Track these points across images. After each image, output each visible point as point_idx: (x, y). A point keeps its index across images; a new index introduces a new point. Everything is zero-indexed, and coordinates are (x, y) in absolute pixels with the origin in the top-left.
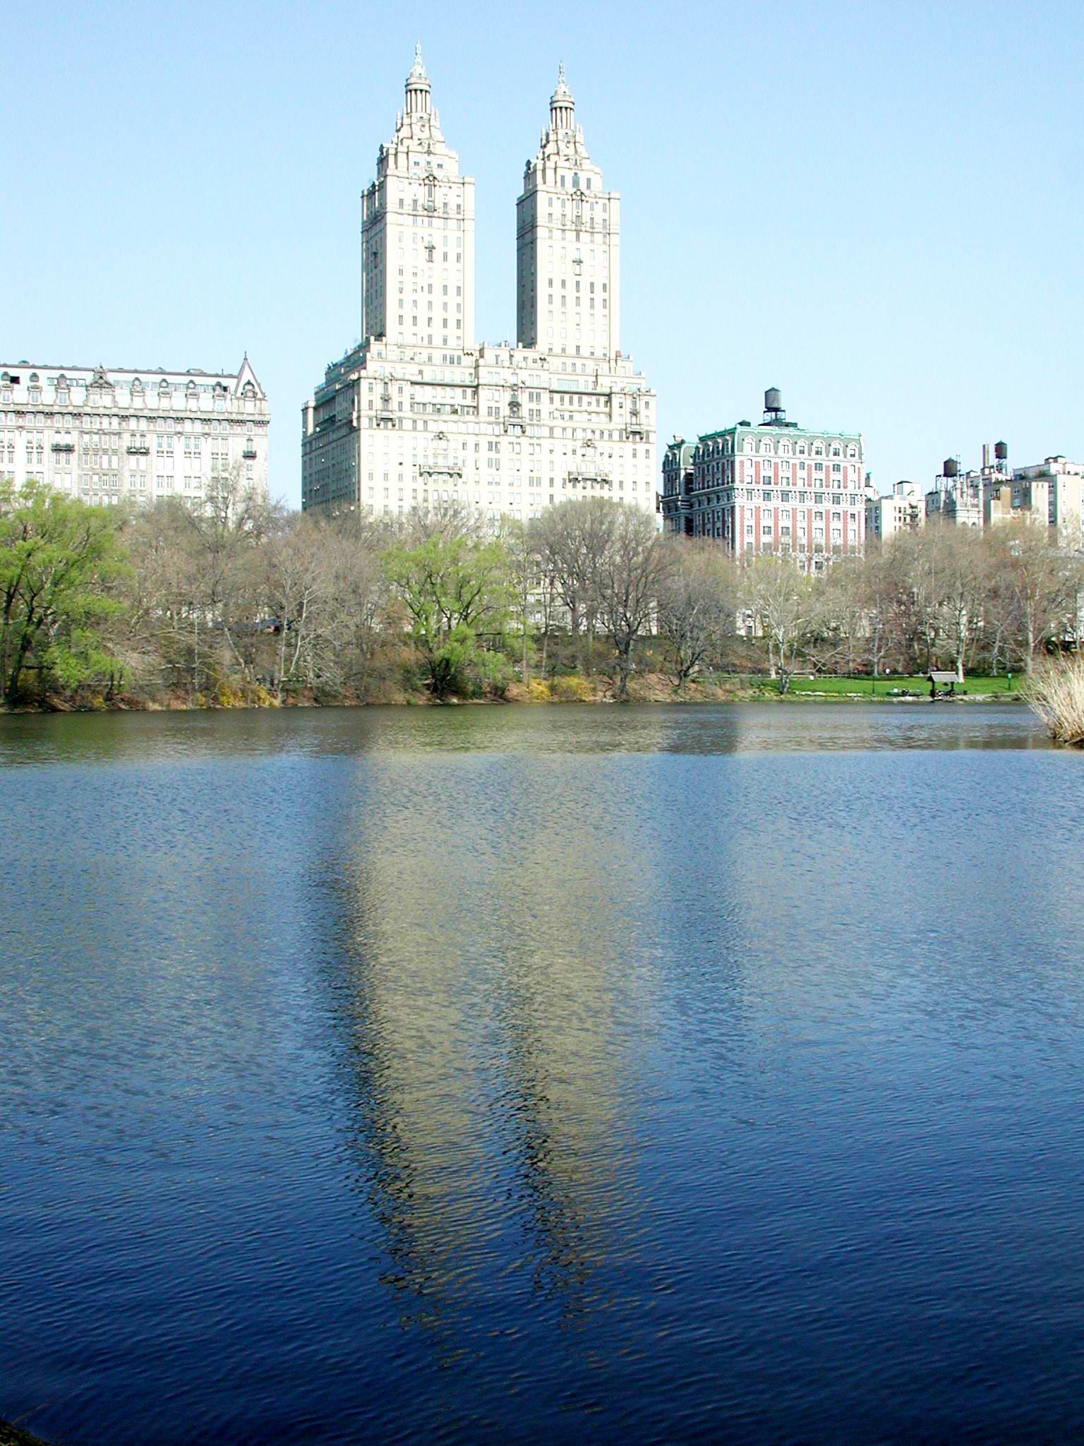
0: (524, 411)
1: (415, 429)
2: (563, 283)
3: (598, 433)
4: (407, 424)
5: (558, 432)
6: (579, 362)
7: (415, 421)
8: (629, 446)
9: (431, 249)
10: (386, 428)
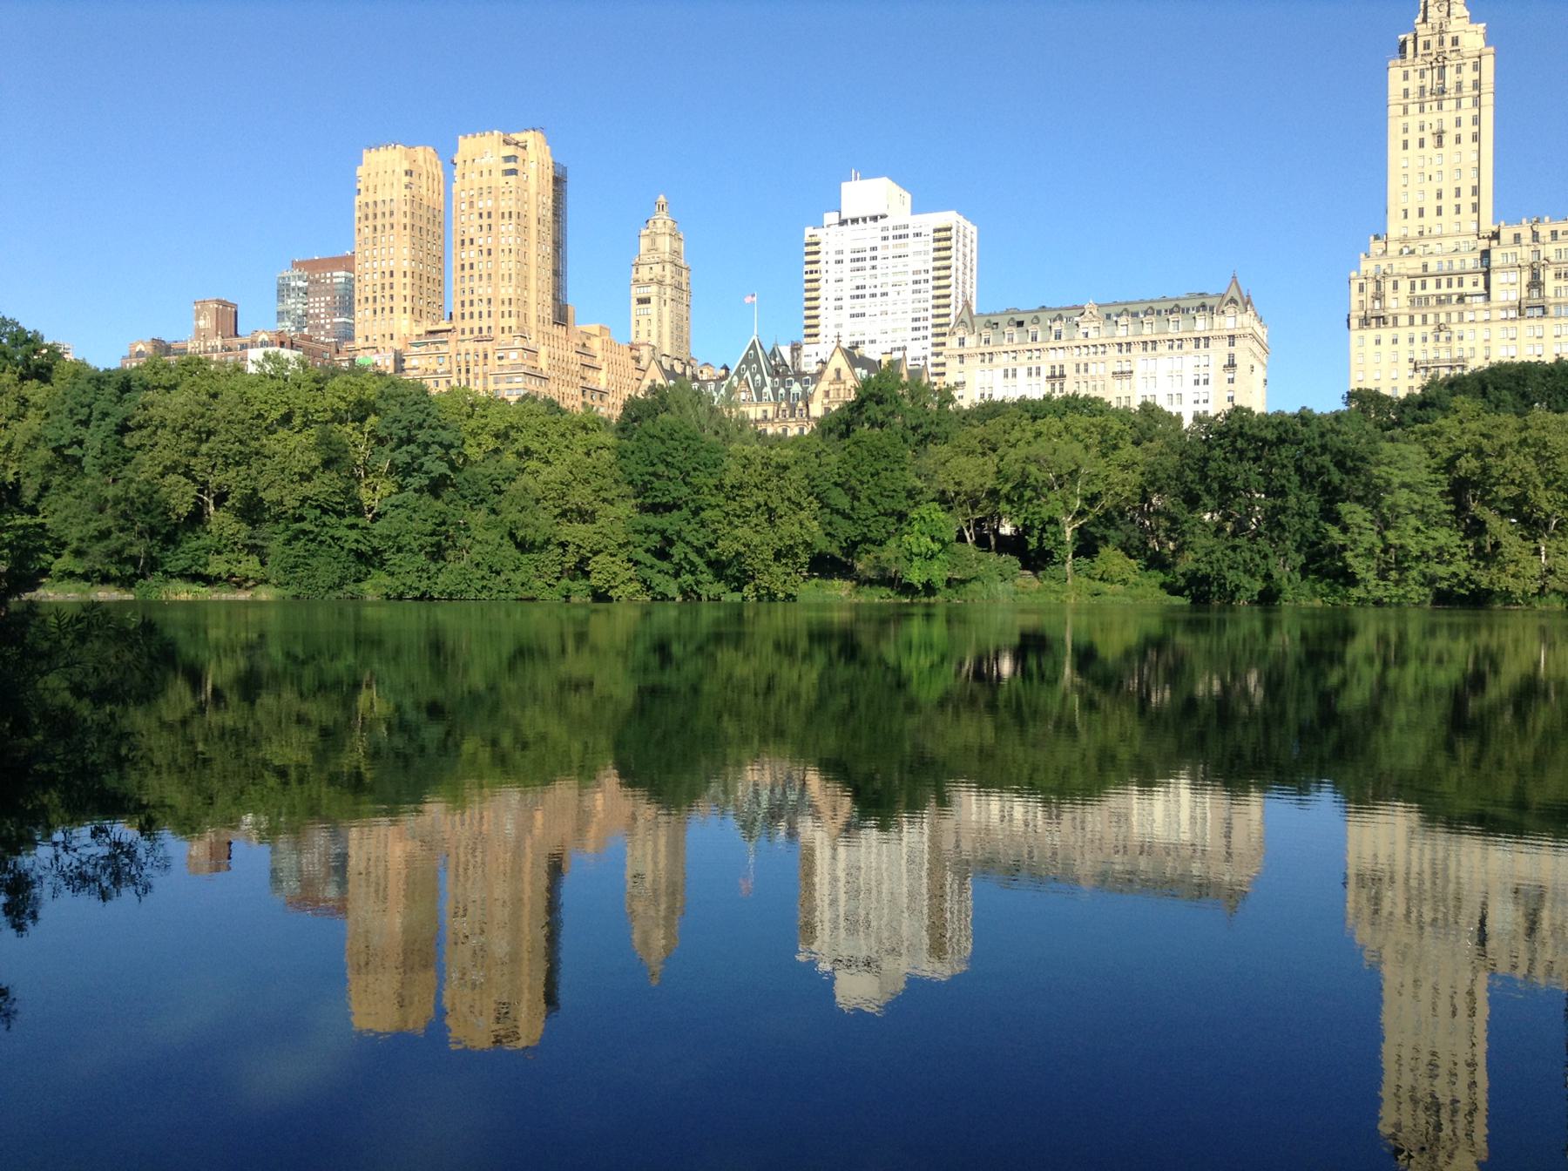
1: (1412, 323)
4: (1403, 320)
7: (1412, 318)
9: (1439, 136)
10: (1378, 326)
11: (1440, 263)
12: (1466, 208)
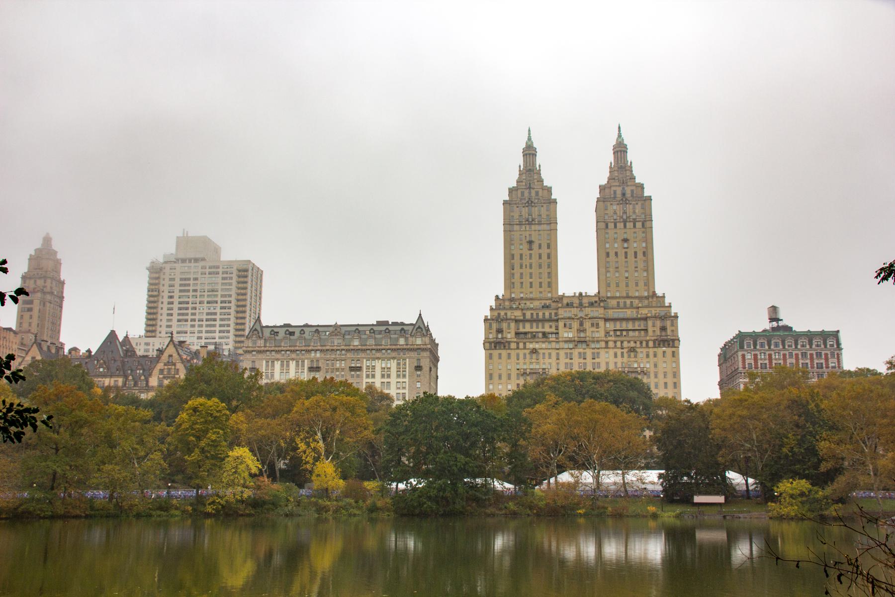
0: (588, 334)
1: (518, 348)
2: (616, 254)
3: (638, 343)
4: (513, 345)
5: (611, 344)
6: (628, 301)
7: (518, 343)
8: (660, 351)
9: (531, 242)
11: (532, 314)
12: (545, 285)
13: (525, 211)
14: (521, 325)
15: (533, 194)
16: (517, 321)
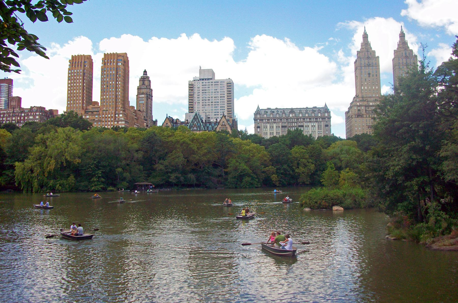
4: (365, 116)
9: (369, 74)
13: (366, 61)
14: (367, 108)
15: (369, 54)
16: (366, 106)
